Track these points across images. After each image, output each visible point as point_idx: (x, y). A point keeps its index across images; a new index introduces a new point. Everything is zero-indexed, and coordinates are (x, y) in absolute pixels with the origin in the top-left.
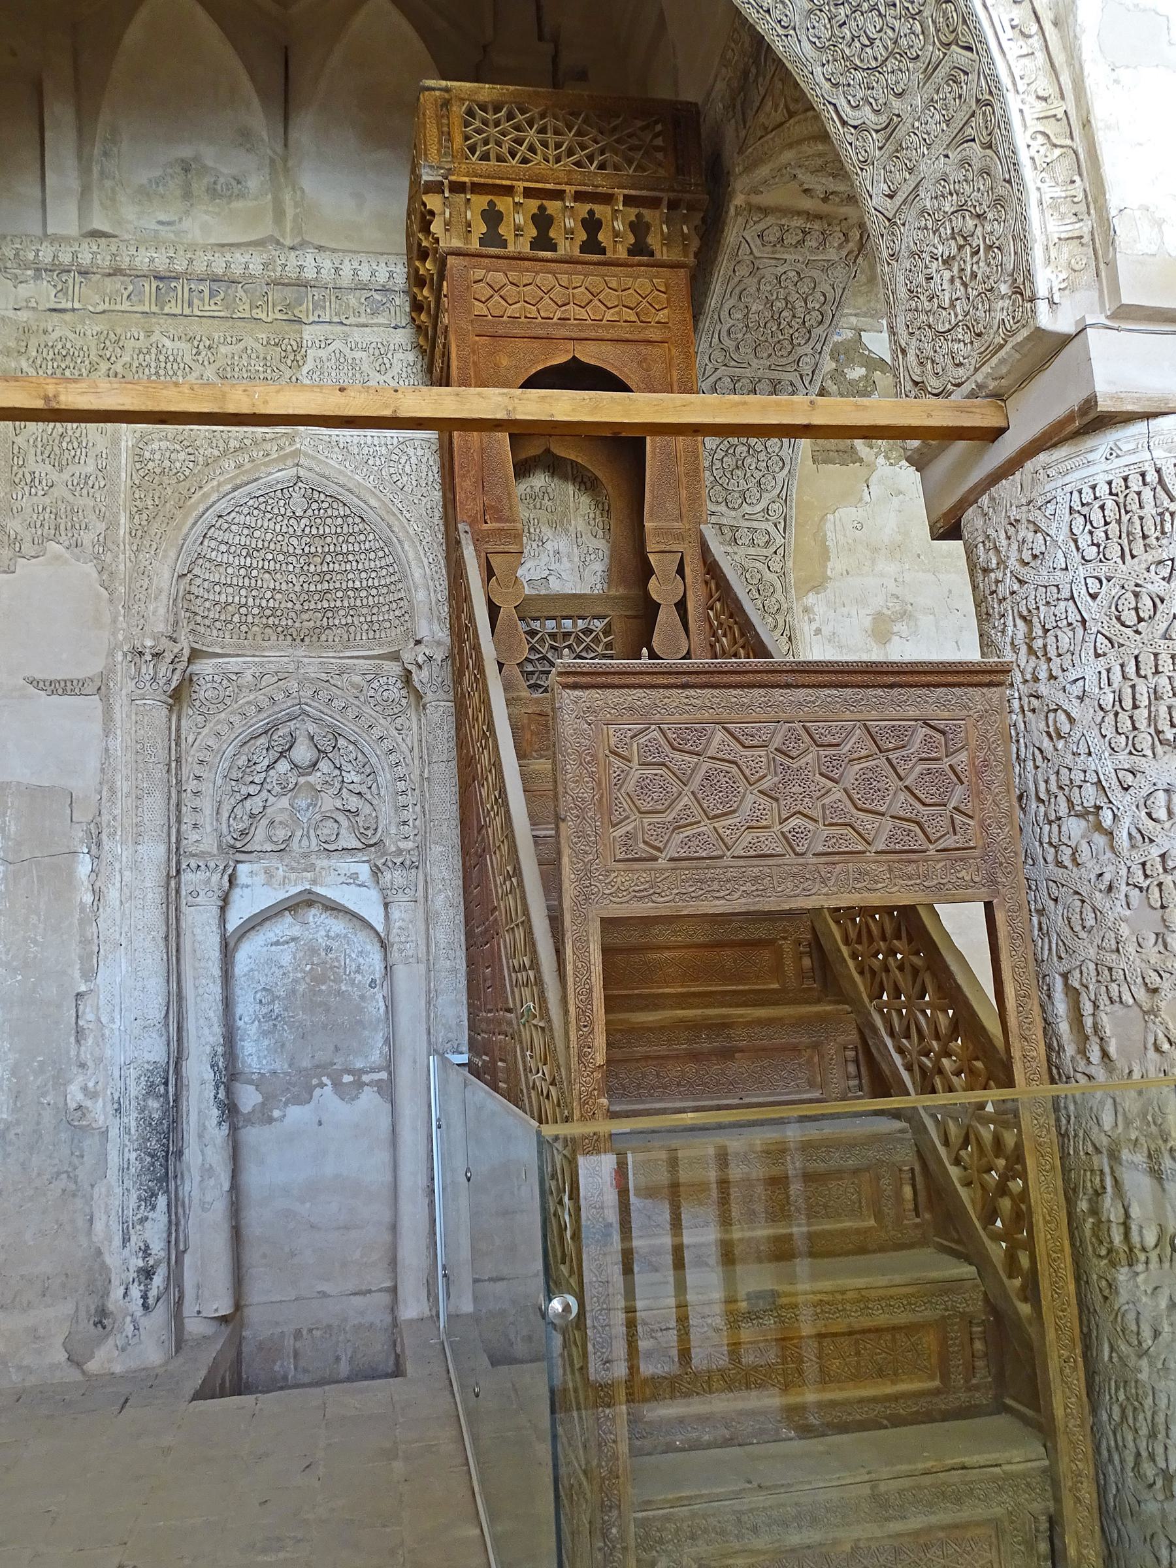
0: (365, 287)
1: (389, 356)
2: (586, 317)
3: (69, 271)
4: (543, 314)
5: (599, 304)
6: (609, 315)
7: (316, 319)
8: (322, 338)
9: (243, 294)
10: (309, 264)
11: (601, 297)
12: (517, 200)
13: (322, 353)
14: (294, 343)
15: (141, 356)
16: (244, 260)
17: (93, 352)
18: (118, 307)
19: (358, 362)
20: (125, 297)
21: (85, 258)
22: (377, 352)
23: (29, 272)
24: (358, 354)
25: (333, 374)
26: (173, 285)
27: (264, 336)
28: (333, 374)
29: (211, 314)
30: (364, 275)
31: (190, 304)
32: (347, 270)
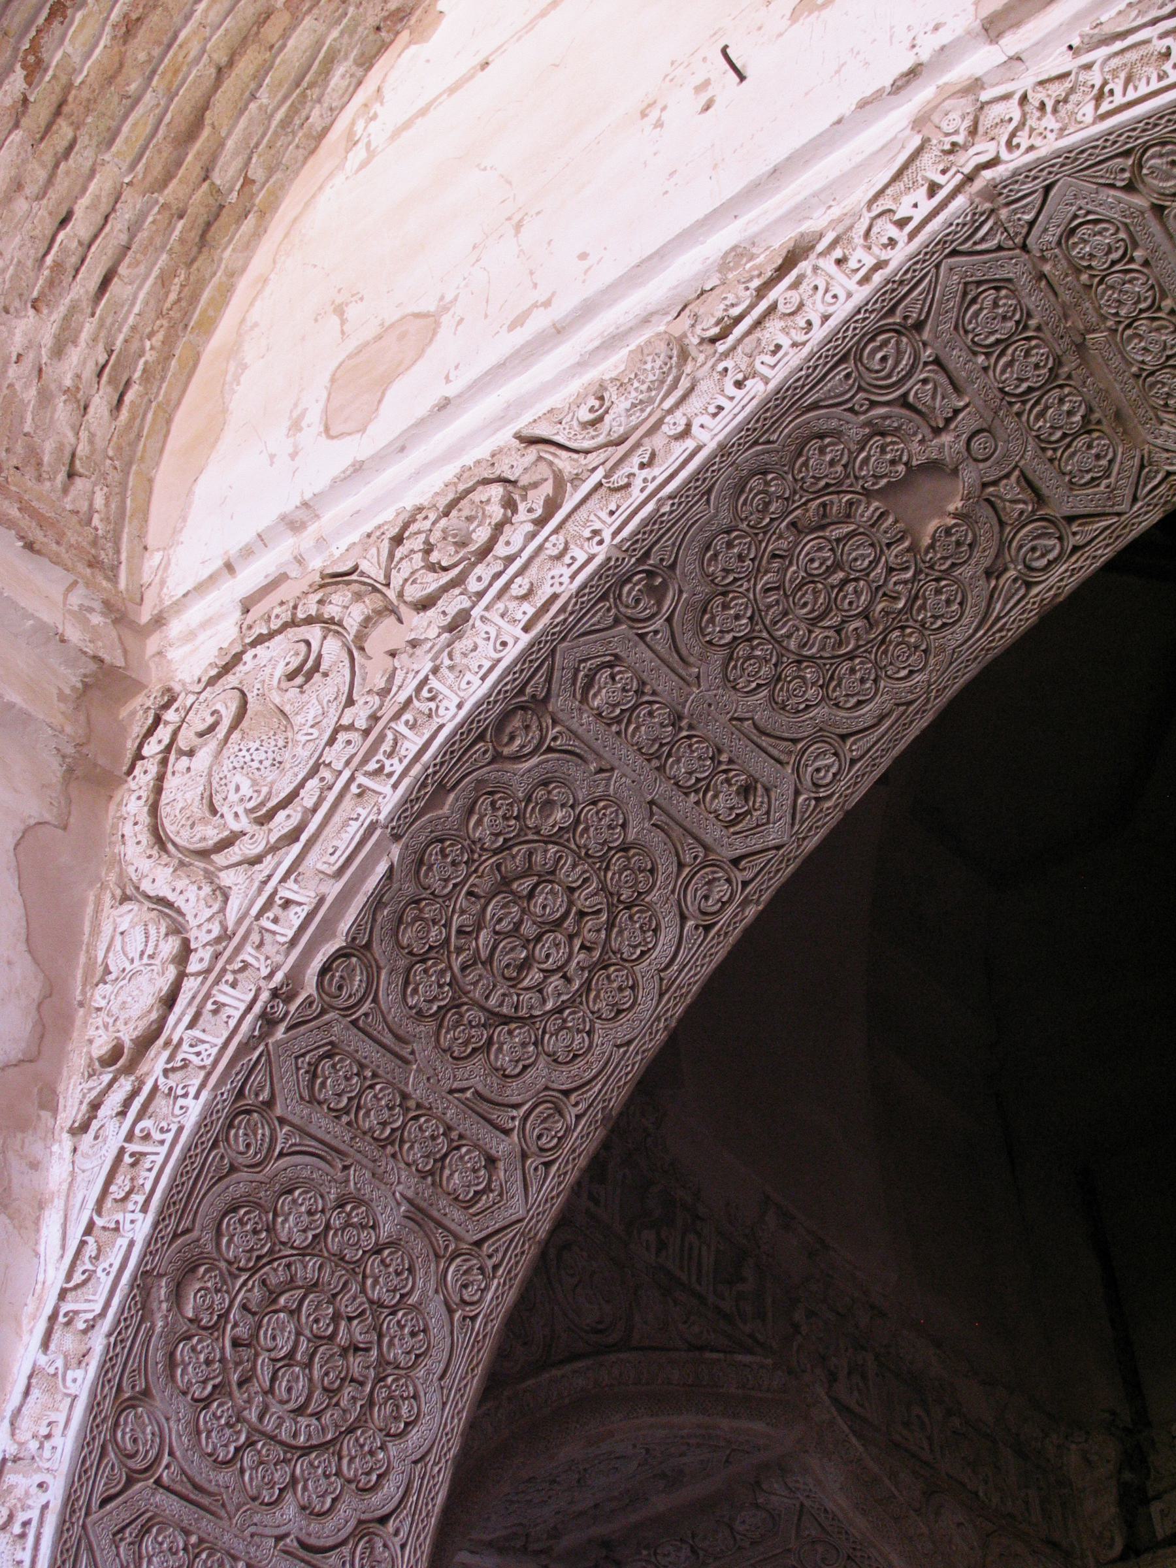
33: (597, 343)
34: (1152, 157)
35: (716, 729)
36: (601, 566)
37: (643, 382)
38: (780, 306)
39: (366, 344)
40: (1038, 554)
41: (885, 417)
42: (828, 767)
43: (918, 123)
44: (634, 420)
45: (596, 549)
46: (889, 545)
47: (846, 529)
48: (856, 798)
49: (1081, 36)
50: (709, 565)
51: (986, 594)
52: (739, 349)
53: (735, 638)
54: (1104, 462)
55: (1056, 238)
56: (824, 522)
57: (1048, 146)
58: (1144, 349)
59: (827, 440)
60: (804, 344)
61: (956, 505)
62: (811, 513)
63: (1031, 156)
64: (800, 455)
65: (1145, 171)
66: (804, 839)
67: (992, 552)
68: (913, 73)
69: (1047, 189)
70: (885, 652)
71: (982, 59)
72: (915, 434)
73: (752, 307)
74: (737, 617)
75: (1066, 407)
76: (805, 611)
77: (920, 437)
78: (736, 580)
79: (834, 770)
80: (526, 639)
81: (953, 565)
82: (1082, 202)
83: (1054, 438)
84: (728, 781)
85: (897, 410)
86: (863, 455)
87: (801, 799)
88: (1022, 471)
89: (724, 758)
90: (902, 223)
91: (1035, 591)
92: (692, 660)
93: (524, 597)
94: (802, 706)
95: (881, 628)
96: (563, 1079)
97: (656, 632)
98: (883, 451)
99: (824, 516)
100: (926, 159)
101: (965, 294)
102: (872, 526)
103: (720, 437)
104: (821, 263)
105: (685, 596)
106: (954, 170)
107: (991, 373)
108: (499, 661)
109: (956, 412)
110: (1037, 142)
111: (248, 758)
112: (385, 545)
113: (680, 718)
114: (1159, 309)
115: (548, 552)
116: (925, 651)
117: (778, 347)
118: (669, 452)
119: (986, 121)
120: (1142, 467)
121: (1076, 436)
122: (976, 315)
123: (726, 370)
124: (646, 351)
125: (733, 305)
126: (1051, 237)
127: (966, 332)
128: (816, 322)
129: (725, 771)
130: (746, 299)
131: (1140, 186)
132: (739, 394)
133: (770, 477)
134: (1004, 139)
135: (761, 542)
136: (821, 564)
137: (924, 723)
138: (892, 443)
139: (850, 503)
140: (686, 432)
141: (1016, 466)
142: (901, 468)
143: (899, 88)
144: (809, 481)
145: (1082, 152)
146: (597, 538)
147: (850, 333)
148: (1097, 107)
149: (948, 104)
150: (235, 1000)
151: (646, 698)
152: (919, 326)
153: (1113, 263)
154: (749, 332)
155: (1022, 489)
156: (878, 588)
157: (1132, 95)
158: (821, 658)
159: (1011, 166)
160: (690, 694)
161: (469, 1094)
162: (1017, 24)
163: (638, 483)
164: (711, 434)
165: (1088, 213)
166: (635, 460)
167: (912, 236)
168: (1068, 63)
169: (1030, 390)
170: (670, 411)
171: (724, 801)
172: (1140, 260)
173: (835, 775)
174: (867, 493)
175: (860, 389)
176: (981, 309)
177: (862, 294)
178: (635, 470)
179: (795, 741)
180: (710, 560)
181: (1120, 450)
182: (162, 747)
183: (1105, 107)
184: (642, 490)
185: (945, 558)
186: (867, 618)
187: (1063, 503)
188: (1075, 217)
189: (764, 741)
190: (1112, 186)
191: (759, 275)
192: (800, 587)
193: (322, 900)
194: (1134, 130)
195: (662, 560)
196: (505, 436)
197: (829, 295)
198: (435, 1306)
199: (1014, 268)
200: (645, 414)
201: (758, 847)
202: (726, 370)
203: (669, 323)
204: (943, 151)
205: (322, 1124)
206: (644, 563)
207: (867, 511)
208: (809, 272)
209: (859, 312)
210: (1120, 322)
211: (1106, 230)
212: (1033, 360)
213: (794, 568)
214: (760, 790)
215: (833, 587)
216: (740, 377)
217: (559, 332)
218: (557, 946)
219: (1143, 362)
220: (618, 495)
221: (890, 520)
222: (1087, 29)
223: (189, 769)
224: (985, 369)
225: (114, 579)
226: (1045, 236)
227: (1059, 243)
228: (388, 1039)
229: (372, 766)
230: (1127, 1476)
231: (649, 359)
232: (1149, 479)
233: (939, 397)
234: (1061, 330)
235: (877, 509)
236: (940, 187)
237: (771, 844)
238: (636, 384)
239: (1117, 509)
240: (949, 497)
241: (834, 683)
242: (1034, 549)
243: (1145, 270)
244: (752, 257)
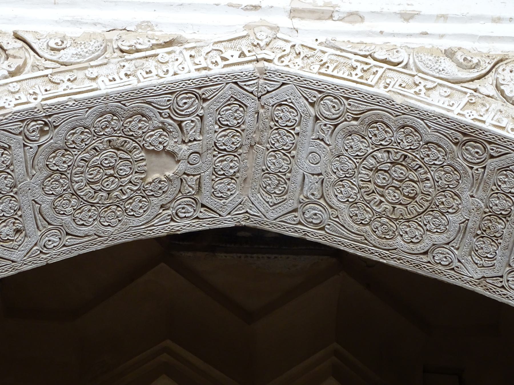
33: (69, 19)
34: (328, 100)
35: (25, 200)
36: (31, 109)
37: (86, 48)
38: (159, 57)
40: (183, 211)
41: (170, 125)
42: (54, 242)
43: (247, 27)
44: (73, 60)
46: (136, 172)
47: (126, 156)
48: (55, 260)
49: (326, 40)
50: (69, 135)
51: (156, 213)
52: (133, 62)
53: (58, 170)
54: (229, 193)
55: (273, 103)
56: (121, 148)
57: (294, 70)
58: (274, 163)
59: (144, 119)
60: (162, 78)
61: (169, 173)
62: (119, 141)
63: (286, 69)
64: (131, 117)
65: (322, 102)
66: (25, 264)
67: (169, 199)
68: (256, 8)
69: (283, 84)
70: (105, 211)
71: (283, 21)
72: (175, 138)
73: (147, 50)
74: (64, 162)
75: (232, 164)
76: (90, 176)
77: (176, 140)
78: (74, 148)
79: (55, 244)
81: (153, 195)
82: (292, 97)
83: (219, 173)
84: (14, 223)
85: (175, 125)
86: (153, 133)
87: (35, 248)
88: (200, 177)
89: (19, 213)
90: (224, 59)
91: (172, 223)
92: (36, 167)
94: (62, 212)
95: (111, 201)
97: (31, 148)
98: (161, 135)
99: (122, 146)
100: (244, 41)
101: (229, 100)
102: (136, 161)
103: (109, 91)
104: (184, 52)
105: (52, 141)
106: (254, 53)
107: (216, 134)
109: (195, 140)
110: (291, 65)
113: (15, 187)
114: (290, 153)
115: (10, 88)
116: (119, 221)
117: (150, 72)
118: (82, 82)
119: (273, 44)
120: (240, 203)
121: (227, 177)
122: (227, 110)
123: (124, 66)
124: (92, 37)
125: (140, 44)
126: (272, 102)
127: (219, 114)
128: (171, 72)
129: (16, 219)
130: (147, 45)
131: (316, 106)
132: (125, 79)
133: (115, 118)
135: (94, 140)
136: (109, 163)
137: (99, 248)
138: (165, 136)
139: (135, 148)
141: (200, 174)
142: (161, 147)
143: (247, 9)
144: (127, 129)
145: (305, 80)
146: (34, 96)
147: (181, 85)
148: (319, 69)
149: (263, 28)
151: (8, 171)
152: (205, 100)
153: (287, 126)
154: (140, 58)
155: (196, 184)
156: (121, 186)
157: (335, 73)
158: (82, 198)
159: (277, 67)
160: (25, 180)
162: (302, 18)
163: (63, 86)
164: (105, 87)
165: (291, 102)
166: (67, 76)
167: (225, 66)
168: (314, 45)
169: (225, 150)
170: (92, 67)
172: (296, 131)
173: (54, 246)
174: (143, 147)
175: (169, 108)
176: (230, 109)
177: (195, 74)
178: (65, 80)
179: (49, 224)
180: (71, 134)
181: (237, 193)
183: (323, 70)
184: (64, 90)
185: (152, 191)
186: (109, 194)
187: (205, 198)
188: (286, 101)
189: (39, 216)
190: (307, 100)
191: (157, 40)
192: (95, 166)
194: (329, 86)
195: (54, 122)
196: (10, 29)
197: (181, 67)
199: (251, 103)
200: (79, 61)
201: (6, 257)
202: (124, 66)
203: (103, 31)
204: (253, 44)
206: (47, 118)
207: (139, 154)
208: (178, 52)
209: (189, 80)
210: (272, 148)
211: (293, 113)
212: (233, 140)
213: (98, 158)
214: (23, 235)
215: (106, 174)
216: (129, 73)
217: (55, 4)
219: (269, 167)
220: (52, 85)
221: (144, 163)
222: (330, 38)
224: (216, 132)
226: (270, 100)
227: (273, 106)
231: (94, 41)
232: (239, 209)
233: (193, 130)
234: (250, 136)
235: (142, 156)
236: (245, 56)
237: (12, 259)
238: (83, 47)
239: (221, 213)
240: (168, 169)
241: (79, 211)
242: (183, 208)
243: (295, 136)
244: (152, 30)
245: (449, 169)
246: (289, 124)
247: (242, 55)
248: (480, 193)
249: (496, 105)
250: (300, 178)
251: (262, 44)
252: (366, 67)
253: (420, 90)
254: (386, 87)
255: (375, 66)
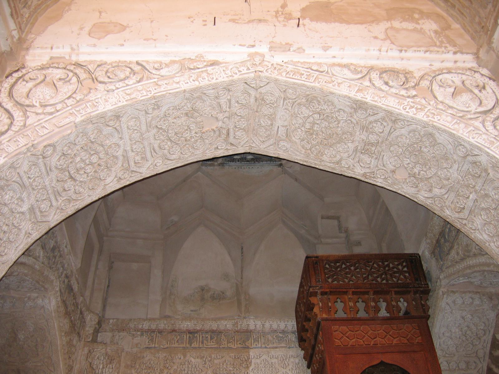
0: (275, 331)
1: (287, 360)
2: (385, 343)
3: (154, 332)
4: (366, 343)
5: (390, 337)
6: (395, 342)
7: (255, 346)
8: (258, 354)
9: (224, 337)
10: (253, 323)
11: (391, 333)
12: (350, 296)
13: (258, 361)
14: (246, 357)
15: (181, 366)
16: (225, 324)
17: (162, 365)
18: (173, 346)
19: (273, 364)
20: (176, 341)
21: (162, 326)
22: (282, 359)
23: (139, 333)
24: (274, 360)
25: (263, 370)
26: (195, 335)
27: (233, 354)
28: (263, 370)
29: (211, 346)
30: (275, 326)
31: (202, 343)
32: (267, 325)
36: (149, 98)
39: (105, 23)
45: (149, 94)
60: (210, 81)
63: (270, 75)
73: (202, 68)
80: (125, 103)
82: (273, 89)
93: (128, 94)
96: (74, 197)
108: (117, 104)
110: (272, 74)
111: (45, 91)
112: (96, 66)
132: (193, 82)
134: (266, 69)
140: (178, 83)
146: (150, 92)
150: (22, 141)
157: (294, 77)
161: (55, 189)
164: (184, 87)
165: (273, 92)
167: (240, 75)
171: (138, 158)
182: (19, 76)
183: (288, 76)
193: (53, 130)
197: (219, 76)
198: (24, 232)
202: (192, 76)
205: (25, 179)
216: (194, 79)
218: (90, 168)
223: (25, 85)
225: (22, 34)
228: (48, 169)
229: (77, 109)
230: (97, 326)
236: (250, 70)
245: (349, 121)
246: (271, 102)
247: (248, 69)
248: (364, 132)
249: (371, 90)
250: (276, 128)
251: (257, 64)
252: (308, 74)
253: (335, 84)
254: (319, 83)
255: (313, 73)
